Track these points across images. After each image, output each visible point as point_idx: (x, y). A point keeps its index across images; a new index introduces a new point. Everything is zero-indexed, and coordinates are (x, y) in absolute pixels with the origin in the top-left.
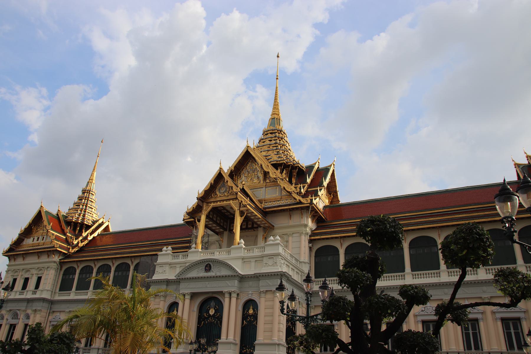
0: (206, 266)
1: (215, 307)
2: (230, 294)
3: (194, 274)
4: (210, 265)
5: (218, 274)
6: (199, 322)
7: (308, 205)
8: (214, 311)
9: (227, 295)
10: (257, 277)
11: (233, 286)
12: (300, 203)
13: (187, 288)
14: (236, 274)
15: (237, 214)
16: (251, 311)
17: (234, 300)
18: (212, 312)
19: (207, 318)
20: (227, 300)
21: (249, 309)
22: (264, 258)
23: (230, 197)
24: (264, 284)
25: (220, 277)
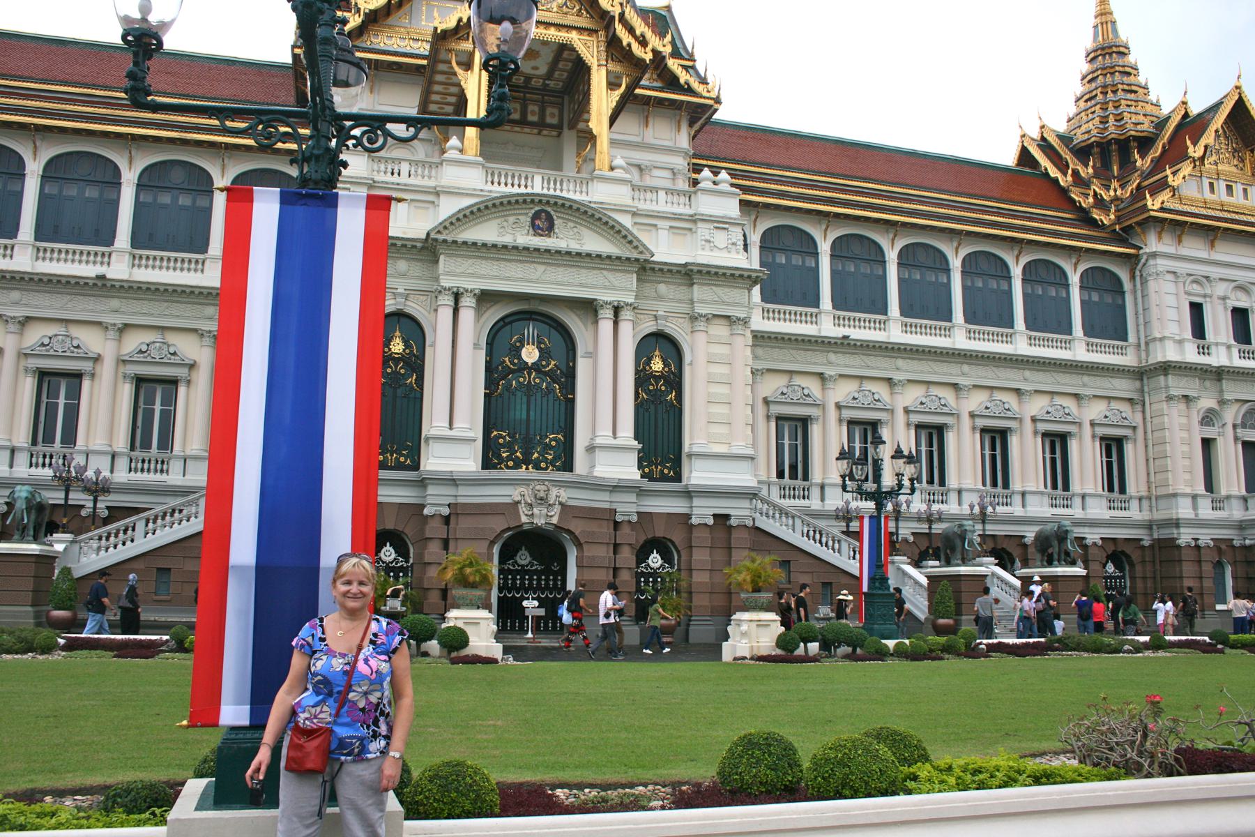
0: (536, 216)
1: (539, 343)
2: (617, 310)
3: (487, 232)
4: (548, 213)
5: (574, 246)
6: (490, 382)
7: (711, 102)
8: (536, 354)
9: (607, 313)
10: (688, 274)
11: (613, 288)
12: (689, 90)
13: (456, 273)
14: (635, 255)
15: (598, 79)
16: (657, 365)
17: (626, 328)
18: (530, 354)
19: (513, 372)
20: (606, 326)
21: (650, 360)
22: (700, 225)
23: (572, 20)
24: (706, 297)
25: (579, 254)
